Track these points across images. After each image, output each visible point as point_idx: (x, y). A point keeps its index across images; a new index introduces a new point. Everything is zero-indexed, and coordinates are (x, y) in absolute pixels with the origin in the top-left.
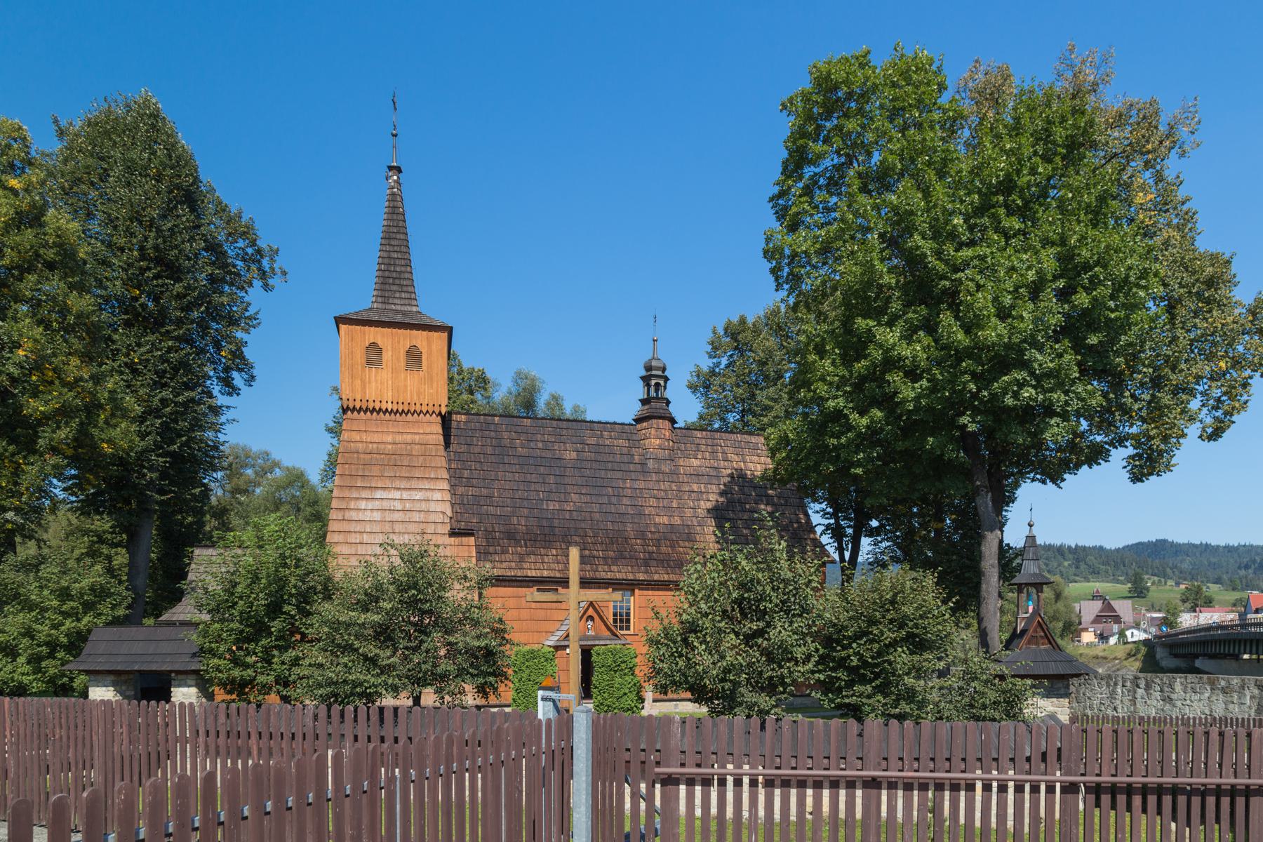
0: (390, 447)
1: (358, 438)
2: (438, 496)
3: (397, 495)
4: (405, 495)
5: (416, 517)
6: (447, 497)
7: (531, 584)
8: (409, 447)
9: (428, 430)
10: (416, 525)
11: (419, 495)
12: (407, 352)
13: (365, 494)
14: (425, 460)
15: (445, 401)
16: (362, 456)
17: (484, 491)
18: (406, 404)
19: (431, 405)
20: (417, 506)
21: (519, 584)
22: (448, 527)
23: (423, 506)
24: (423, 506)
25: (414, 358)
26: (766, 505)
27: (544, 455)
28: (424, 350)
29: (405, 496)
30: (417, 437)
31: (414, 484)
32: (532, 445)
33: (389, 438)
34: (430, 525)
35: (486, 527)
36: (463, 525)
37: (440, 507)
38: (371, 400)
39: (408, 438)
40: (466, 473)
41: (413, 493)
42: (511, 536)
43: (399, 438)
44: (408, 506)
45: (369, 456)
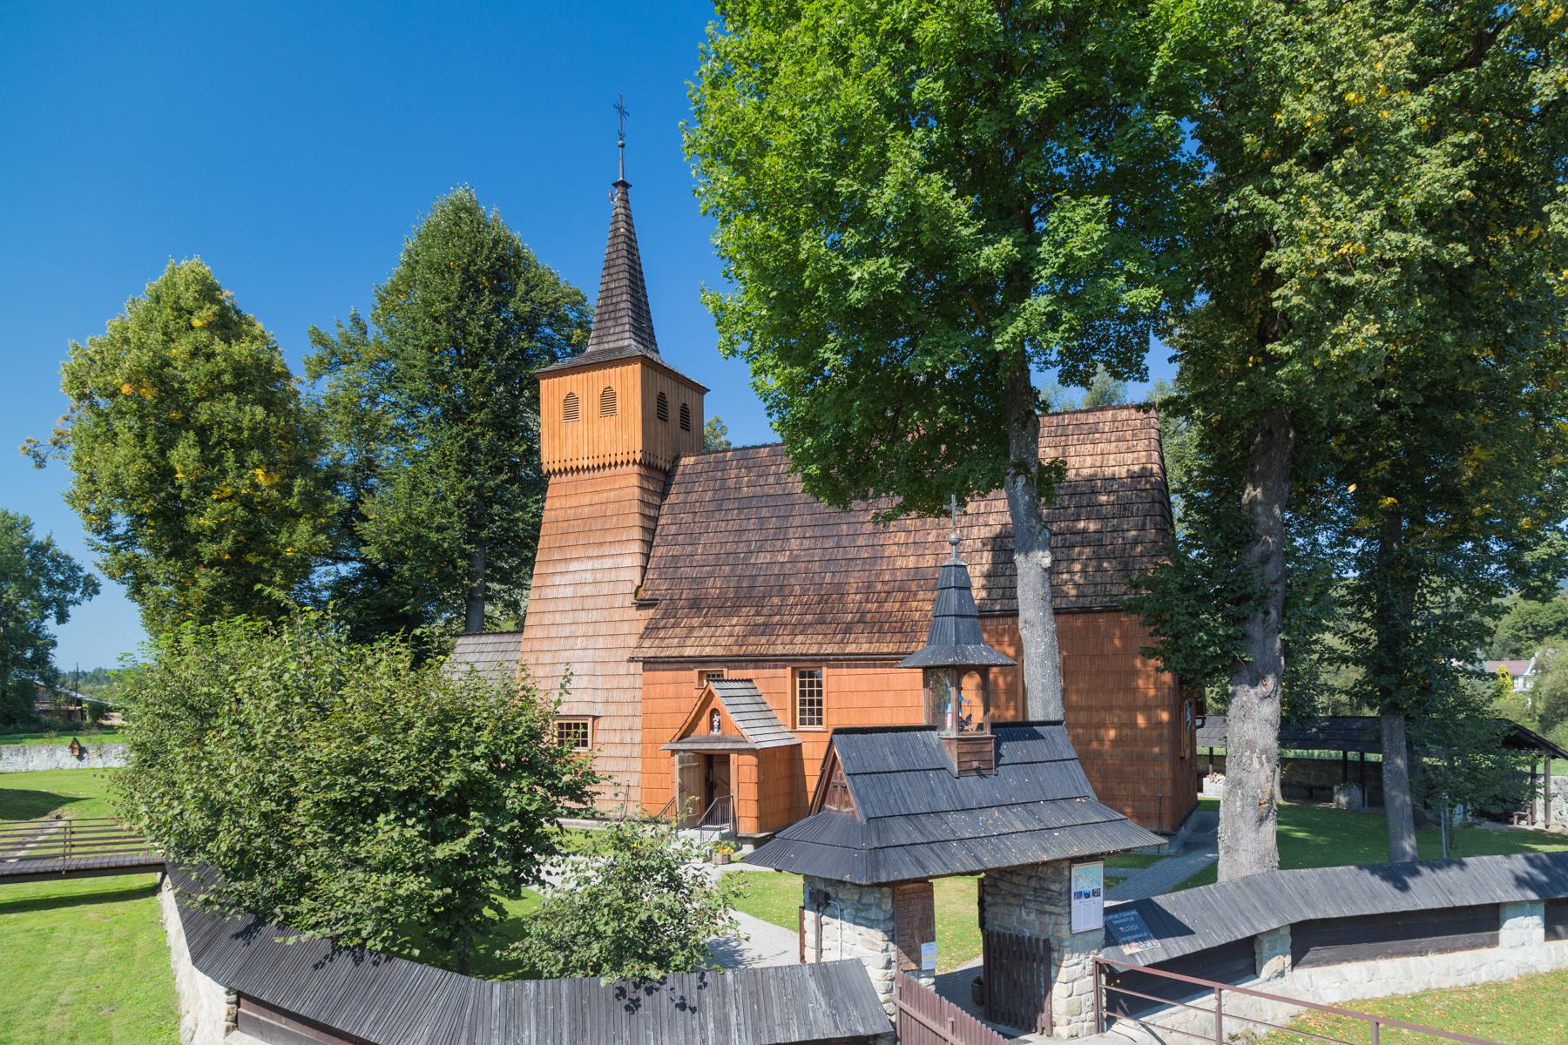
0: (586, 510)
1: (558, 506)
2: (628, 561)
3: (589, 564)
4: (597, 564)
5: (606, 589)
6: (638, 561)
8: (604, 507)
10: (605, 598)
11: (608, 563)
13: (560, 568)
15: (639, 447)
16: (561, 524)
17: (689, 549)
21: (679, 666)
22: (631, 599)
24: (613, 575)
25: (608, 400)
26: (1088, 519)
28: (618, 391)
29: (596, 566)
30: (612, 494)
31: (606, 550)
33: (587, 500)
35: (672, 595)
36: (648, 595)
37: (625, 575)
39: (604, 497)
40: (673, 529)
41: (604, 560)
43: (596, 499)
44: (599, 577)
45: (566, 524)
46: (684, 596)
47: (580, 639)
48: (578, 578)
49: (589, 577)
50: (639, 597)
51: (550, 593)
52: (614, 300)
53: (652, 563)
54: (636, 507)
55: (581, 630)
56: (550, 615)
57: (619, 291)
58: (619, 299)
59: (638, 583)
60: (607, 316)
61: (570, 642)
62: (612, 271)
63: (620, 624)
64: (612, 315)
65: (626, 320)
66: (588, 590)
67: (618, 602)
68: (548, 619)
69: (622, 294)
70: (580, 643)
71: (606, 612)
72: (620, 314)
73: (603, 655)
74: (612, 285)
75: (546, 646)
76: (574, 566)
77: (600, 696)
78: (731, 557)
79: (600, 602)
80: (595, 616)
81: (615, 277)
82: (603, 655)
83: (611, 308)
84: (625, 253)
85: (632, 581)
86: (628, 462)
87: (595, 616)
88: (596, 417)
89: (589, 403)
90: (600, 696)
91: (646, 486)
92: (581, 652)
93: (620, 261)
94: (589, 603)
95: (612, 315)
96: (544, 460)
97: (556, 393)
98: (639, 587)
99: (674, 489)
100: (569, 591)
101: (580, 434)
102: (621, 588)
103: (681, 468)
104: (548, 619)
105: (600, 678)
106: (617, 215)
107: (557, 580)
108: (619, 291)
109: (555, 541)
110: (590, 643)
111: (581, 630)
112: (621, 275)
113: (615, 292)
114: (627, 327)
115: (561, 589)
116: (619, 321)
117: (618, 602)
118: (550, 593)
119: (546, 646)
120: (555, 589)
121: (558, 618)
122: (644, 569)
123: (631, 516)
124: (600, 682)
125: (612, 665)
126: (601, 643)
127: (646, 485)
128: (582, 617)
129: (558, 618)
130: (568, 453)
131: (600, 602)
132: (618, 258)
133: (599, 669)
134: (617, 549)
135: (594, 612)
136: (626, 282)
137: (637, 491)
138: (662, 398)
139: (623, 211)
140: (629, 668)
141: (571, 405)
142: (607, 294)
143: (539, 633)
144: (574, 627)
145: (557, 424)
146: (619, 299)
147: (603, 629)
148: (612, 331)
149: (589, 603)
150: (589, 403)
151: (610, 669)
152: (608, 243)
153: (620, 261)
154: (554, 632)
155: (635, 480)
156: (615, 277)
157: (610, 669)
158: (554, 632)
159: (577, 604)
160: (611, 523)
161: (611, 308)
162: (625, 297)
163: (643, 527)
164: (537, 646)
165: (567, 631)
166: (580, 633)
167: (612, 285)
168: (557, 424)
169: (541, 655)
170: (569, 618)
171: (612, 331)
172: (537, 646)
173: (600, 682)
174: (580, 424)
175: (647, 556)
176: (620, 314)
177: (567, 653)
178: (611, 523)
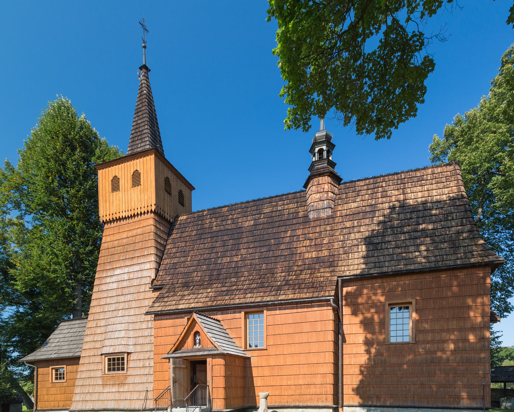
2: (148, 266)
3: (126, 270)
4: (131, 269)
5: (136, 282)
6: (153, 265)
7: (183, 316)
8: (134, 238)
18: (133, 210)
20: (136, 275)
23: (139, 275)
24: (139, 275)
27: (230, 227)
29: (130, 271)
31: (135, 261)
32: (224, 223)
33: (125, 235)
34: (142, 286)
37: (145, 273)
38: (114, 213)
39: (135, 232)
42: (186, 285)
43: (130, 234)
44: (132, 276)
45: (114, 249)
46: (179, 282)
47: (120, 311)
48: (120, 278)
49: (126, 277)
50: (154, 285)
51: (104, 287)
52: (141, 129)
53: (162, 267)
54: (152, 236)
55: (121, 306)
56: (104, 300)
57: (143, 124)
58: (143, 128)
59: (153, 277)
60: (136, 138)
61: (115, 313)
62: (139, 114)
63: (143, 301)
64: (140, 137)
65: (147, 139)
66: (125, 284)
67: (142, 288)
68: (103, 302)
69: (144, 126)
70: (120, 313)
71: (135, 295)
72: (144, 136)
73: (134, 319)
74: (139, 122)
75: (102, 316)
76: (118, 272)
77: (131, 341)
78: (207, 261)
79: (132, 290)
80: (129, 297)
81: (141, 117)
82: (134, 319)
83: (139, 134)
84: (146, 104)
86: (148, 211)
87: (129, 297)
89: (125, 182)
90: (131, 341)
91: (158, 226)
92: (121, 318)
93: (144, 108)
94: (126, 291)
95: (140, 137)
96: (101, 215)
98: (153, 280)
100: (115, 286)
101: (121, 198)
102: (144, 281)
104: (103, 302)
105: (132, 332)
106: (142, 84)
107: (108, 280)
108: (143, 124)
110: (127, 313)
111: (121, 306)
112: (144, 115)
113: (141, 125)
114: (148, 143)
115: (111, 285)
116: (143, 140)
117: (142, 288)
118: (104, 287)
119: (102, 316)
120: (107, 285)
121: (108, 301)
122: (157, 270)
124: (131, 334)
125: (138, 324)
126: (132, 312)
127: (158, 226)
128: (122, 299)
129: (108, 301)
130: (113, 210)
131: (132, 290)
132: (142, 107)
133: (131, 327)
134: (142, 260)
135: (129, 296)
137: (153, 228)
138: (167, 180)
139: (145, 82)
140: (148, 324)
141: (115, 184)
142: (137, 127)
143: (97, 310)
144: (117, 305)
145: (107, 194)
146: (143, 128)
147: (134, 304)
148: (139, 146)
149: (126, 291)
150: (125, 182)
151: (137, 326)
152: (137, 100)
153: (144, 108)
154: (106, 308)
155: (152, 222)
156: (141, 117)
157: (137, 326)
158: (106, 308)
159: (119, 292)
160: (137, 246)
161: (139, 134)
162: (146, 127)
163: (157, 248)
164: (97, 317)
165: (113, 307)
166: (121, 307)
167: (139, 122)
168: (107, 194)
169: (99, 322)
170: (114, 300)
171: (139, 146)
172: (97, 317)
173: (131, 334)
175: (159, 264)
176: (144, 136)
177: (113, 319)
178: (137, 246)
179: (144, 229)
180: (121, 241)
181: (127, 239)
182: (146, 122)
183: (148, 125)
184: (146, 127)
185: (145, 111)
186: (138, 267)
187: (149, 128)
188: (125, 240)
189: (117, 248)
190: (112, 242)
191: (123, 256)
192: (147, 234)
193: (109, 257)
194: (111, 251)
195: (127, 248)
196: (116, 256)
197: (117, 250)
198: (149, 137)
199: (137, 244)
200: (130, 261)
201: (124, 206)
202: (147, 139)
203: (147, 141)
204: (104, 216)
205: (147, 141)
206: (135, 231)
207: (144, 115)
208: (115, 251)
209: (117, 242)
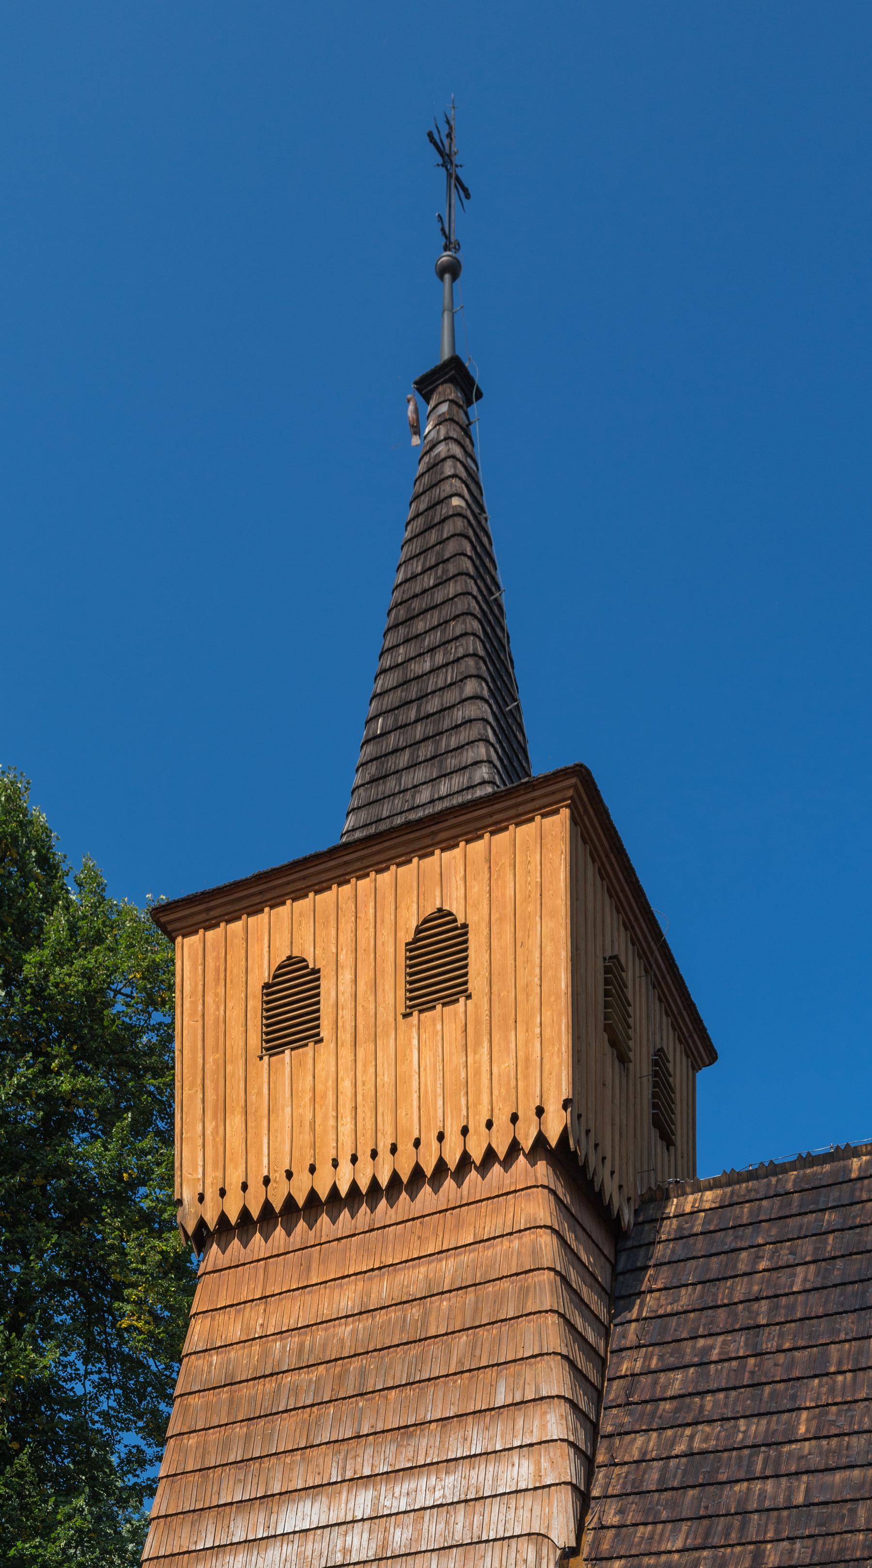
9: (490, 1227)
12: (411, 946)
14: (473, 1345)
18: (406, 1148)
19: (502, 1119)
45: (270, 1385)
85: (540, 1537)
88: (387, 1015)
97: (236, 970)
99: (650, 1279)
103: (669, 1228)
109: (226, 1445)
123: (527, 1326)
136: (472, 645)
137: (546, 1242)
168: (236, 1069)
174: (326, 1050)
179: (486, 1253)
180: (320, 1334)
181: (366, 1322)
182: (471, 662)
183: (479, 677)
184: (470, 687)
185: (461, 605)
186: (450, 1480)
187: (486, 693)
188: (345, 1330)
189: (288, 1378)
190: (256, 1348)
191: (338, 1420)
192: (505, 1284)
193: (240, 1430)
194: (252, 1399)
195: (363, 1373)
196: (288, 1423)
197: (295, 1390)
198: (487, 741)
199: (434, 1348)
200: (390, 1450)
201: (346, 1127)
202: (481, 751)
203: (476, 763)
204: (211, 1194)
205: (476, 763)
206: (421, 1272)
207: (457, 628)
208: (277, 1391)
209: (293, 1341)
